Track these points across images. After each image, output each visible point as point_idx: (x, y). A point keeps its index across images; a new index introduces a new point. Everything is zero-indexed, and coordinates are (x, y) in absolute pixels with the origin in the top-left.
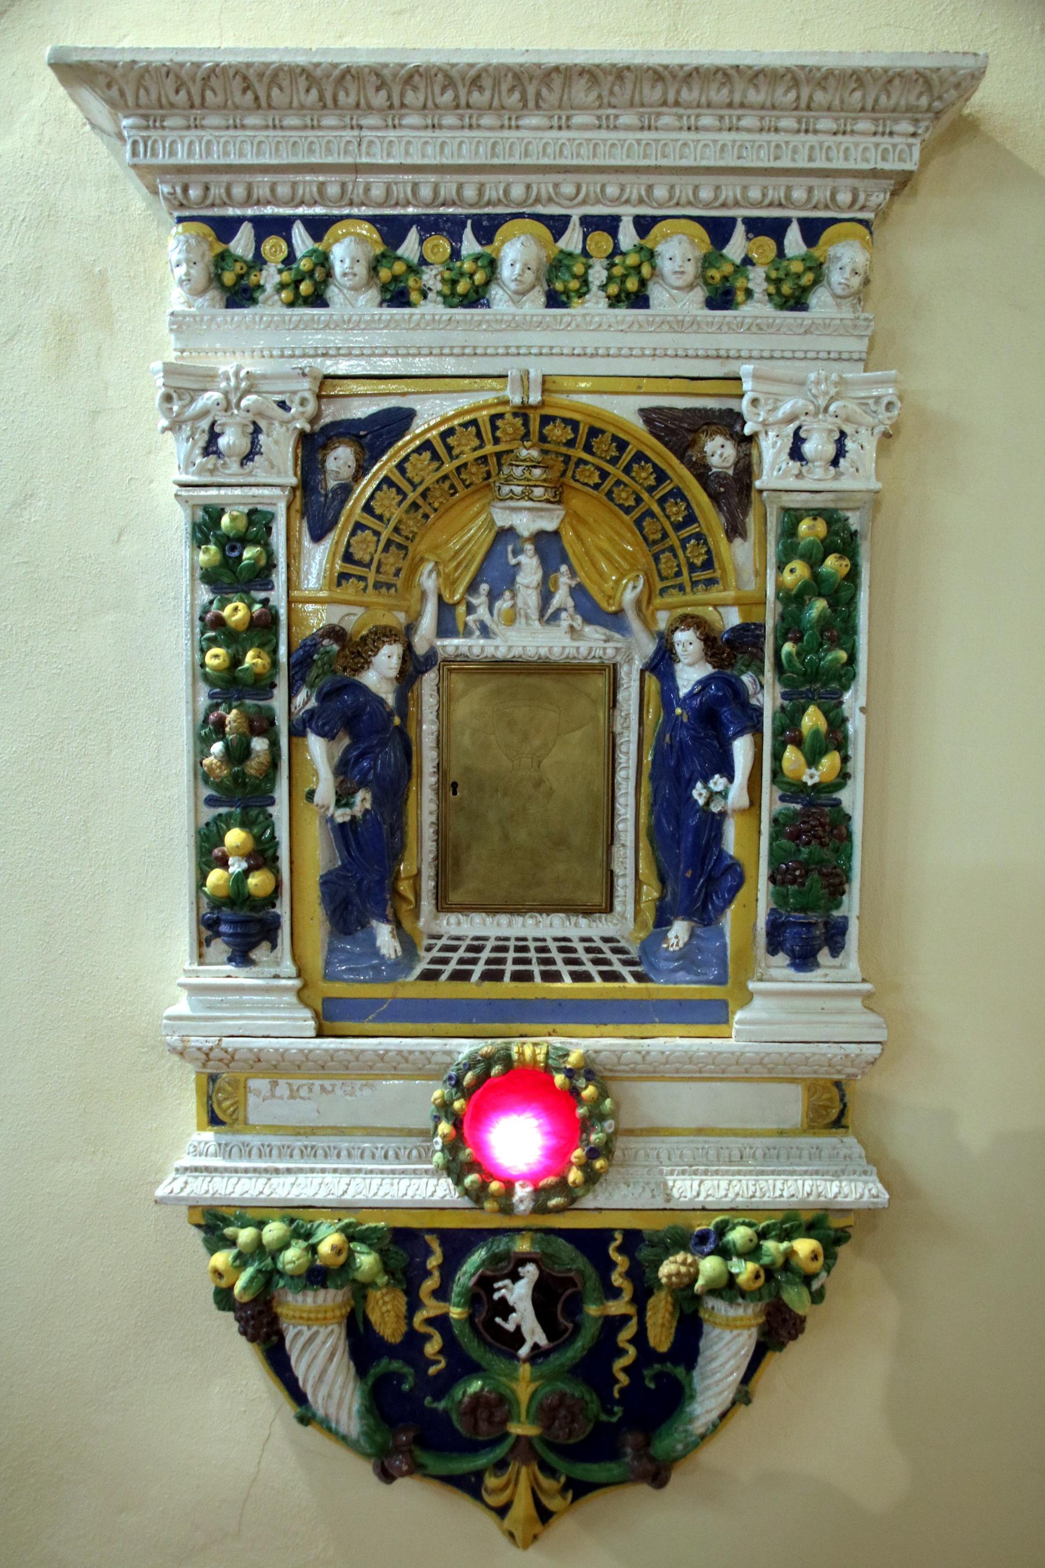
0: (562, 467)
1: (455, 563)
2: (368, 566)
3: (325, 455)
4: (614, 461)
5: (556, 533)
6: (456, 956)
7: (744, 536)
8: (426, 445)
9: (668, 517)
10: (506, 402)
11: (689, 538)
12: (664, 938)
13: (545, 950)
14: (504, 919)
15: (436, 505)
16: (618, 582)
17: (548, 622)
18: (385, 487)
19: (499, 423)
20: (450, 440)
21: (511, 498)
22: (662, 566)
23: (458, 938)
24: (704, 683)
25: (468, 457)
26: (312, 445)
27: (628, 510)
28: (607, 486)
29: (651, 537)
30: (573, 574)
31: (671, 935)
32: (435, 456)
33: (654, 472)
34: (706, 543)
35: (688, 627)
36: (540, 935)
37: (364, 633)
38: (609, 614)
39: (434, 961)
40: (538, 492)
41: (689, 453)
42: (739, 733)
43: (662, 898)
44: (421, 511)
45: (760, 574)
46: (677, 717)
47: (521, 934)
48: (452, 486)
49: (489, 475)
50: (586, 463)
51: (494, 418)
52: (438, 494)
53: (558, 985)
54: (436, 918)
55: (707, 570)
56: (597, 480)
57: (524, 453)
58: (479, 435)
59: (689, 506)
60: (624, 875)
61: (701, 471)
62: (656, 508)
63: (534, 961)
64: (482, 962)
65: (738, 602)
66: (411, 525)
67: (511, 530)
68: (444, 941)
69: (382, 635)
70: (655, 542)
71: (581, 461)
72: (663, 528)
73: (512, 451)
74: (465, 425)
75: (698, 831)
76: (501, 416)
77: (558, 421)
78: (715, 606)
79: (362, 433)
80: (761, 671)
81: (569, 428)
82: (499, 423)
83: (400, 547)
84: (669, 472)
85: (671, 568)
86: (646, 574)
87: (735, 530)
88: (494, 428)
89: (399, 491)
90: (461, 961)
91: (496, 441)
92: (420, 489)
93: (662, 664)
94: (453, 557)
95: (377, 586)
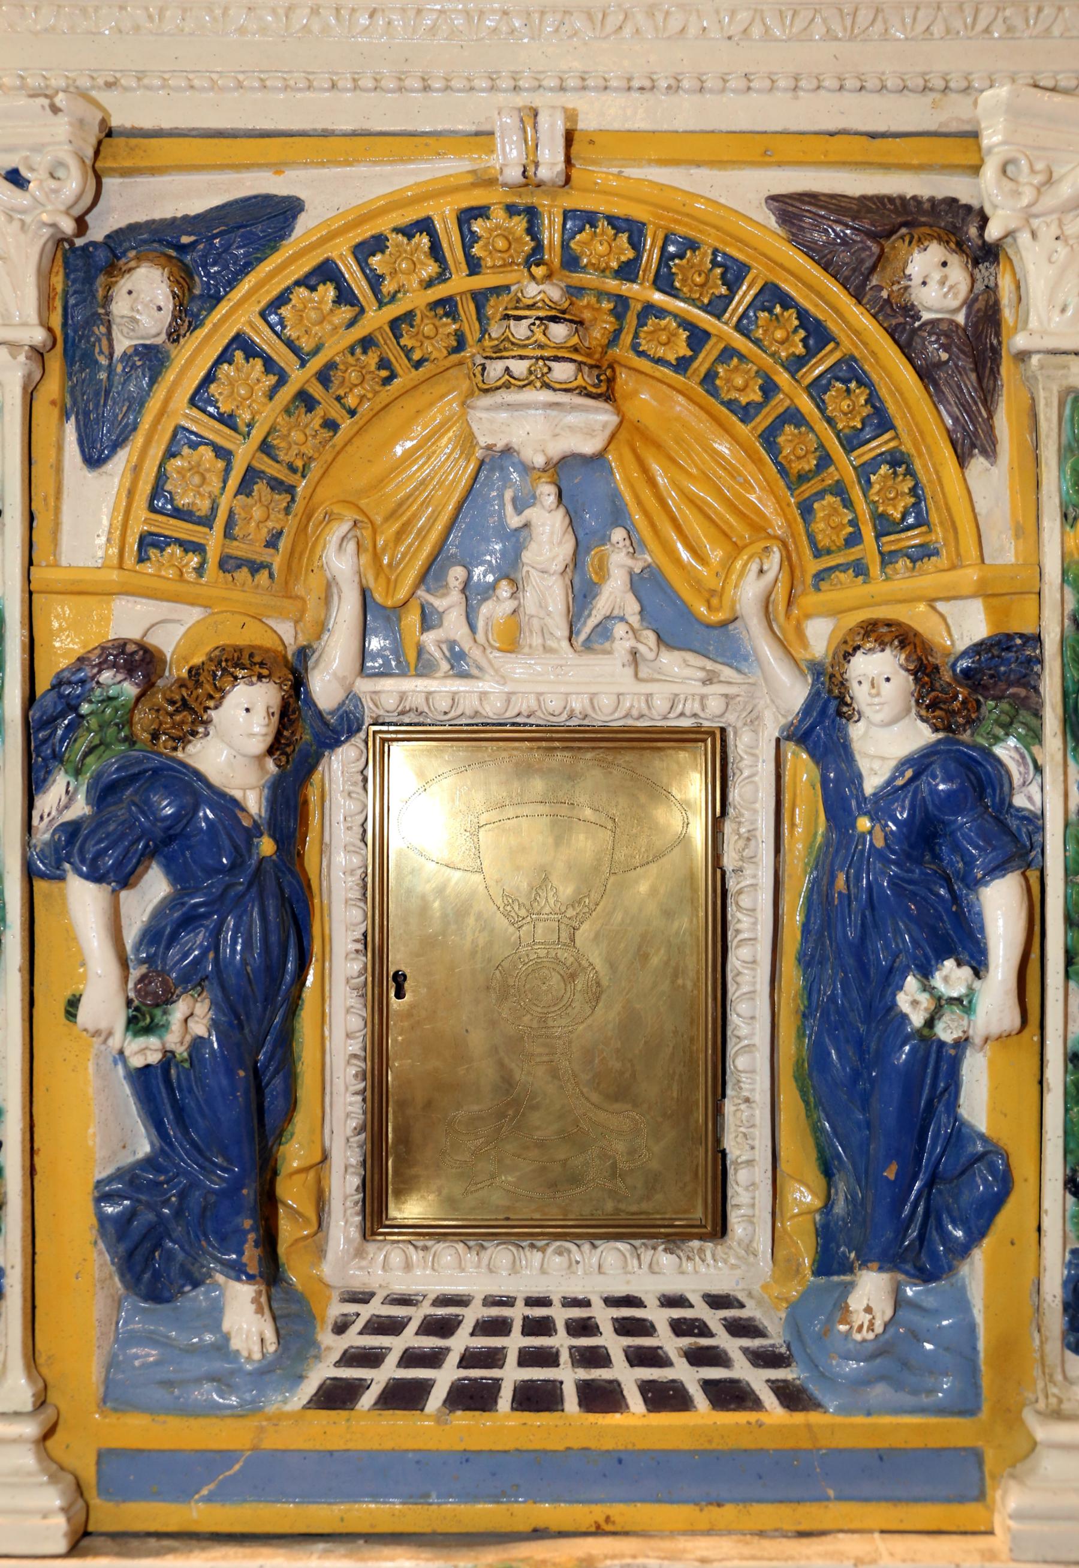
0: (608, 324)
1: (396, 526)
2: (207, 521)
3: (109, 287)
4: (717, 308)
5: (597, 459)
6: (397, 1345)
7: (990, 451)
8: (325, 272)
9: (830, 421)
10: (490, 182)
11: (872, 466)
12: (842, 1310)
13: (584, 1327)
14: (501, 1255)
15: (351, 401)
16: (727, 565)
17: (588, 646)
18: (239, 355)
19: (477, 226)
20: (376, 261)
21: (507, 386)
22: (819, 526)
23: (405, 1301)
24: (920, 764)
25: (416, 299)
26: (83, 268)
27: (746, 413)
28: (703, 363)
29: (796, 467)
30: (636, 545)
31: (857, 1301)
32: (345, 296)
33: (802, 325)
34: (910, 472)
35: (883, 645)
36: (577, 1291)
37: (197, 660)
38: (709, 626)
39: (351, 1358)
40: (563, 371)
41: (874, 281)
42: (998, 870)
43: (828, 1206)
44: (319, 411)
45: (1029, 531)
46: (863, 836)
47: (537, 1289)
48: (384, 363)
49: (460, 344)
50: (660, 312)
51: (467, 216)
52: (354, 376)
53: (615, 1419)
54: (360, 1253)
55: (910, 530)
56: (684, 351)
57: (532, 290)
58: (436, 251)
59: (873, 399)
60: (750, 1163)
61: (901, 322)
62: (806, 405)
63: (564, 1357)
64: (453, 1359)
65: (986, 592)
66: (300, 437)
67: (508, 451)
68: (376, 1308)
69: (233, 663)
70: (803, 478)
71: (650, 310)
72: (821, 446)
73: (507, 288)
74: (407, 232)
75: (912, 1078)
76: (480, 212)
77: (603, 224)
78: (931, 602)
79: (185, 240)
80: (1035, 736)
81: (624, 237)
82: (477, 226)
83: (276, 485)
84: (834, 326)
85: (840, 527)
86: (785, 544)
87: (971, 442)
88: (469, 239)
89: (269, 365)
90: (410, 1359)
91: (474, 266)
92: (316, 364)
93: (824, 723)
94: (392, 515)
95: (227, 564)
